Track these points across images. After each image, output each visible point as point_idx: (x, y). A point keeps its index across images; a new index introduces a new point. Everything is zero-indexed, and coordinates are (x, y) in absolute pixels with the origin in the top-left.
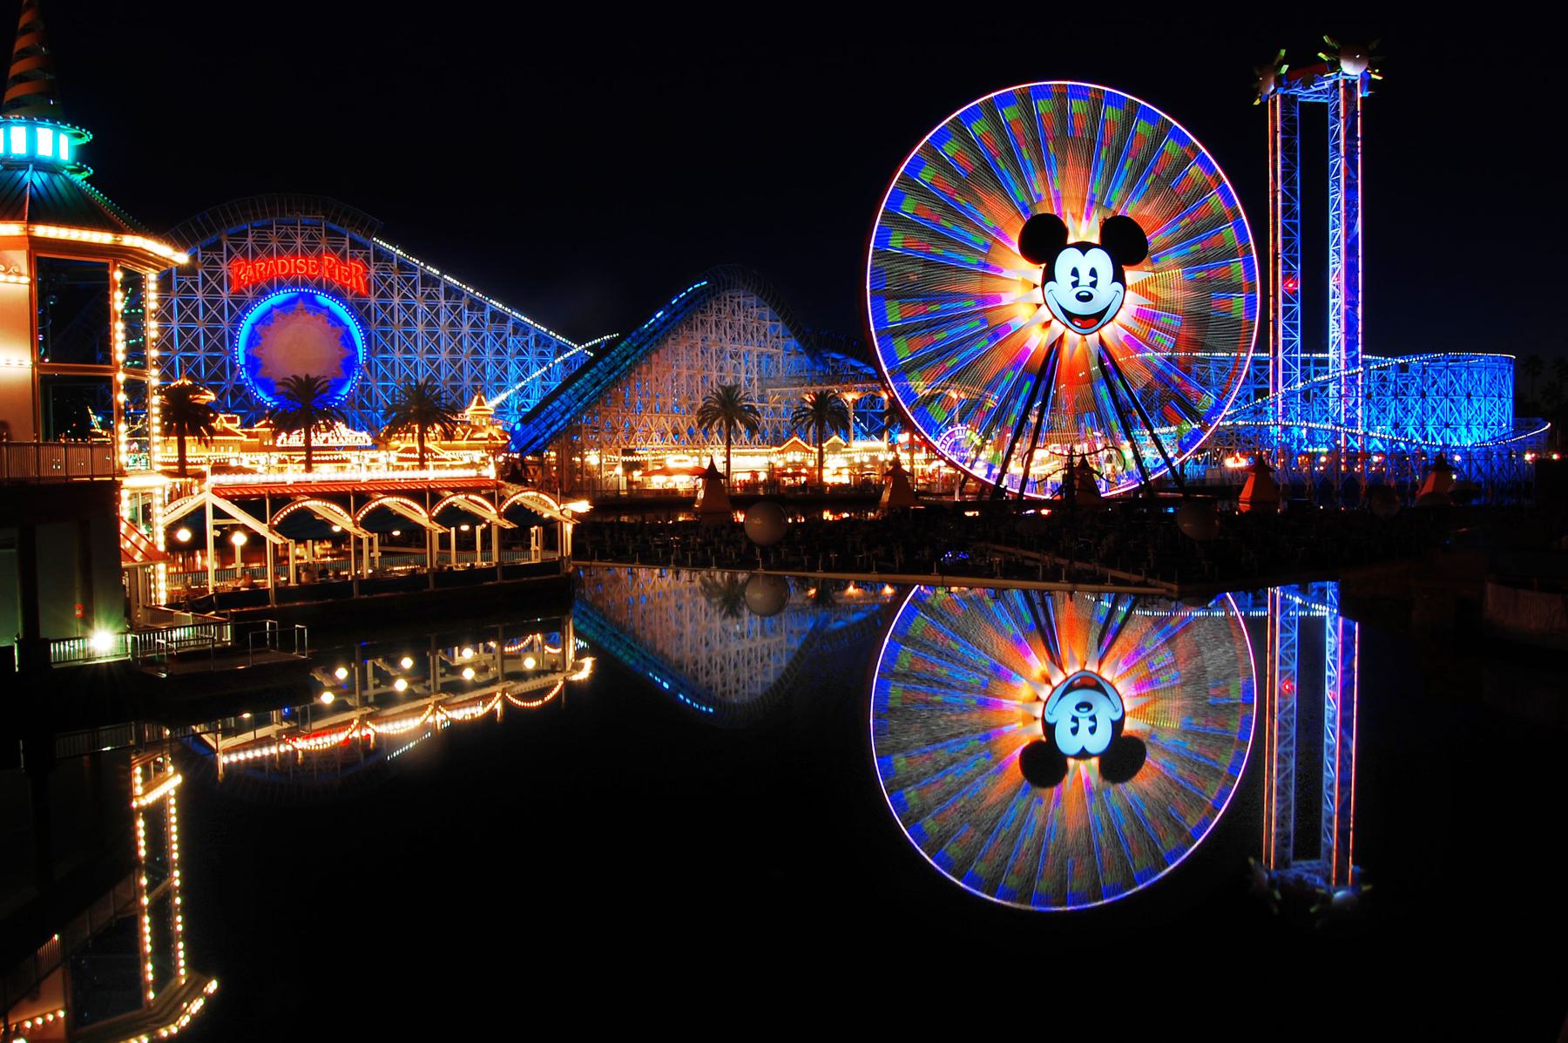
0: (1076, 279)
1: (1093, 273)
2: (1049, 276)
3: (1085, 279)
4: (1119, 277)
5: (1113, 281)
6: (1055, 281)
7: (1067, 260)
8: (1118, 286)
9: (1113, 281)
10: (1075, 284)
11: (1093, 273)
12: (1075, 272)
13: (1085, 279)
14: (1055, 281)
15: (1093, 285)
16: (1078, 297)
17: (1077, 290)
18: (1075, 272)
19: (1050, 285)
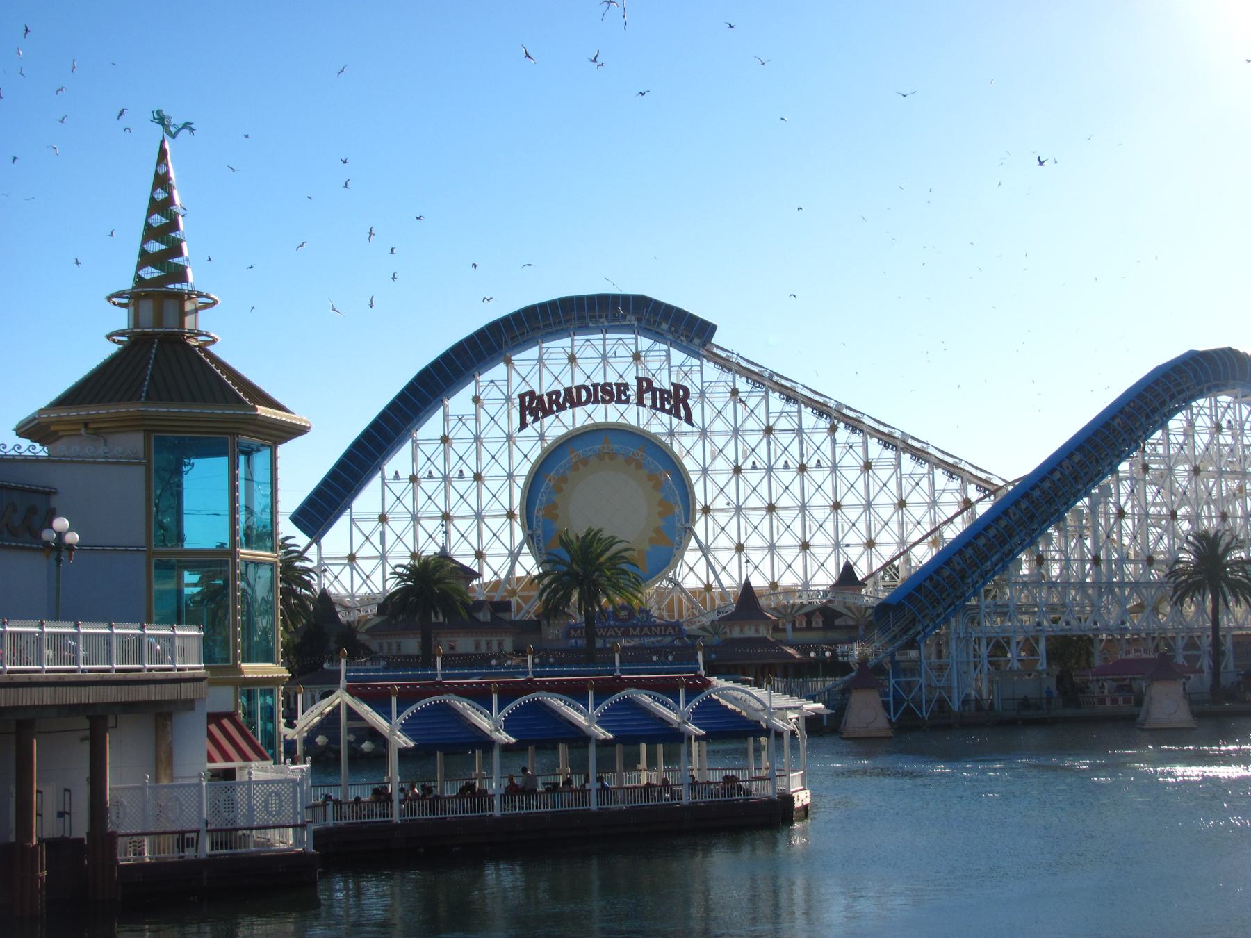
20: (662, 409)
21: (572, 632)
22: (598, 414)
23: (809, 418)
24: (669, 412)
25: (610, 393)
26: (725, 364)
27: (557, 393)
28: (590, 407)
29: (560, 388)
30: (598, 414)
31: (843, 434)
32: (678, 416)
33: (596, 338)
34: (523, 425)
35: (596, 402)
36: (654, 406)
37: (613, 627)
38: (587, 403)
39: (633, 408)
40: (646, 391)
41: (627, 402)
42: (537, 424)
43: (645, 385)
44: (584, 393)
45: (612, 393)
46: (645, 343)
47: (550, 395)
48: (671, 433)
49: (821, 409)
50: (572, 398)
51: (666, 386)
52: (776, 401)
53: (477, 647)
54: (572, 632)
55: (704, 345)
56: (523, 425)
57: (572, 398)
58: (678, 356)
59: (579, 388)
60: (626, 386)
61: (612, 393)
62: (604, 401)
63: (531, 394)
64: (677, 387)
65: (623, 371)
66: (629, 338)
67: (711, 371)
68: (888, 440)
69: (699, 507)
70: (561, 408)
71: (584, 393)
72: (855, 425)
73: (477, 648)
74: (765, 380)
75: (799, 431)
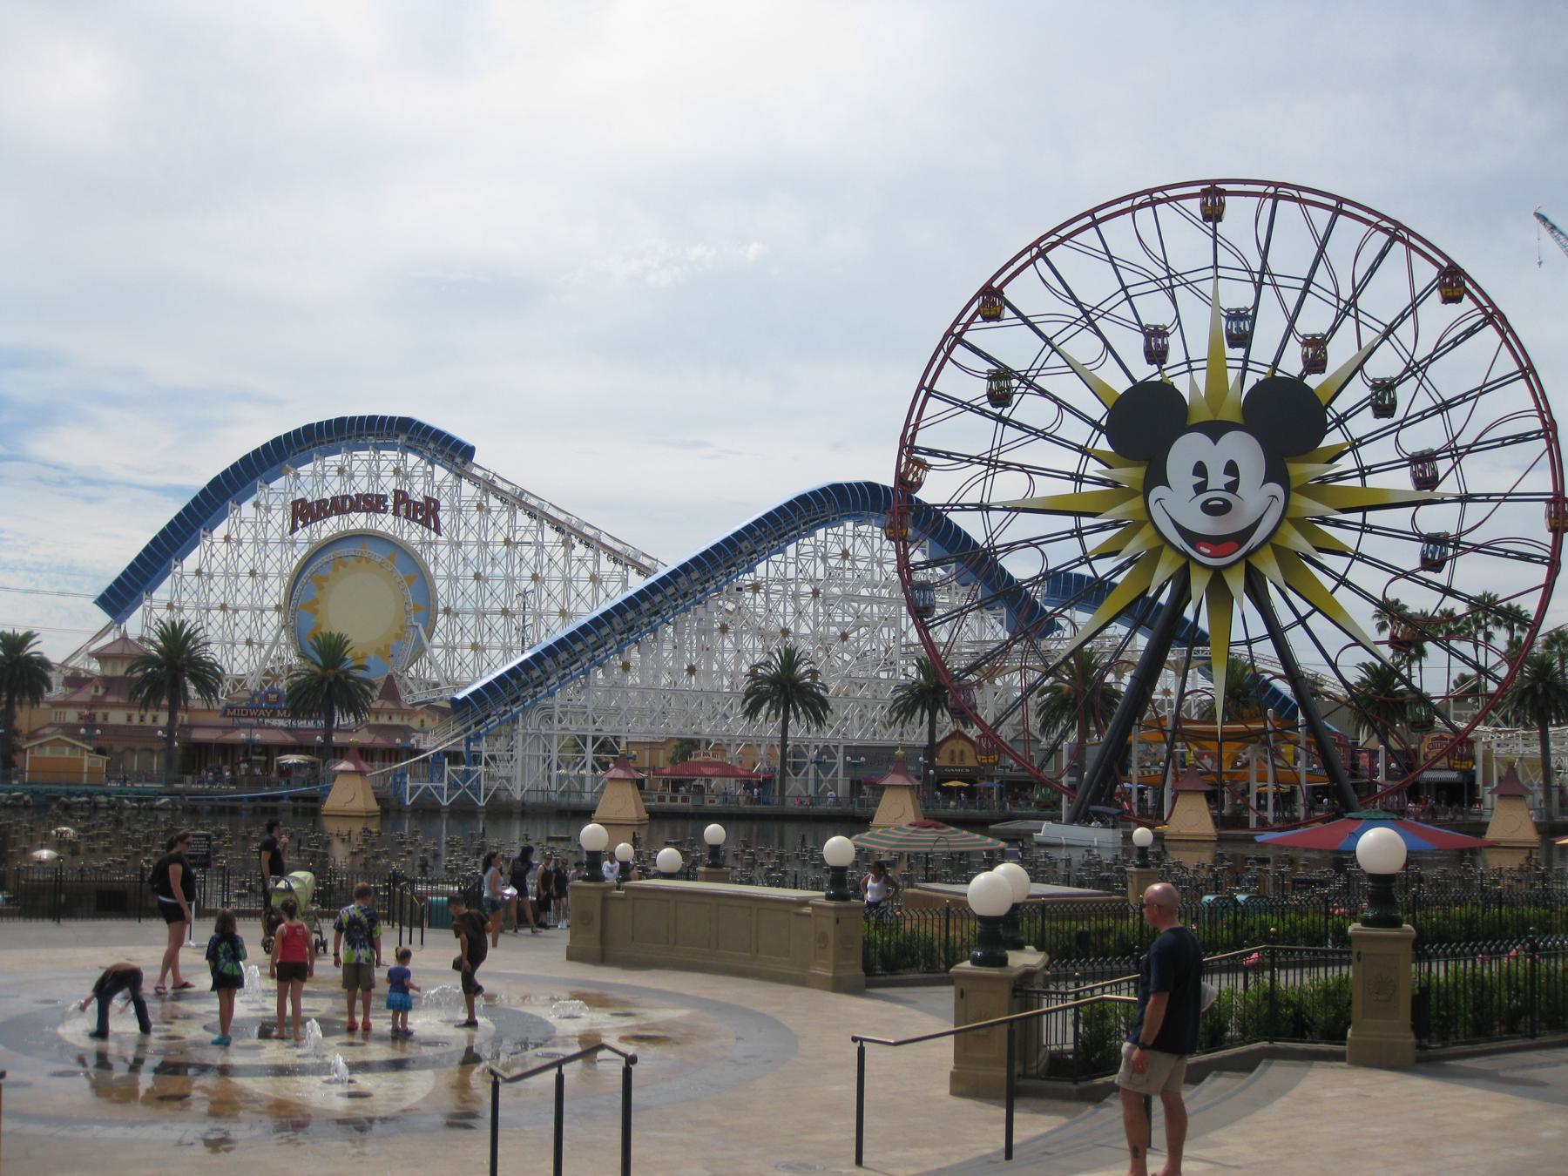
0: (1201, 479)
1: (1231, 468)
2: (1157, 476)
3: (1217, 479)
4: (1275, 472)
5: (1265, 482)
6: (1167, 485)
7: (1186, 451)
8: (1276, 488)
9: (1265, 482)
10: (1200, 488)
11: (1231, 468)
12: (1200, 469)
13: (1217, 479)
14: (1167, 485)
15: (1232, 487)
16: (1207, 508)
17: (1204, 497)
18: (1200, 469)
19: (1157, 492)
20: (415, 519)
21: (229, 710)
22: (359, 521)
23: (551, 535)
24: (419, 522)
25: (370, 503)
26: (474, 479)
27: (325, 501)
28: (353, 515)
29: (327, 496)
30: (359, 521)
31: (580, 550)
32: (427, 525)
33: (364, 455)
34: (294, 529)
35: (358, 510)
36: (407, 517)
37: (264, 709)
38: (349, 511)
39: (390, 518)
40: (402, 503)
41: (385, 511)
42: (307, 530)
43: (401, 497)
44: (348, 503)
45: (372, 504)
46: (412, 459)
47: (318, 502)
48: (422, 543)
49: (558, 527)
50: (339, 506)
51: (420, 499)
52: (522, 519)
53: (129, 718)
54: (229, 710)
55: (464, 463)
56: (294, 529)
57: (339, 506)
58: (440, 472)
59: (344, 497)
60: (385, 497)
61: (372, 504)
62: (365, 510)
63: (303, 501)
64: (428, 499)
65: (388, 485)
66: (392, 455)
67: (468, 489)
68: (616, 557)
69: (441, 607)
70: (328, 515)
71: (348, 503)
72: (588, 542)
73: (142, 721)
74: (516, 500)
75: (540, 546)
